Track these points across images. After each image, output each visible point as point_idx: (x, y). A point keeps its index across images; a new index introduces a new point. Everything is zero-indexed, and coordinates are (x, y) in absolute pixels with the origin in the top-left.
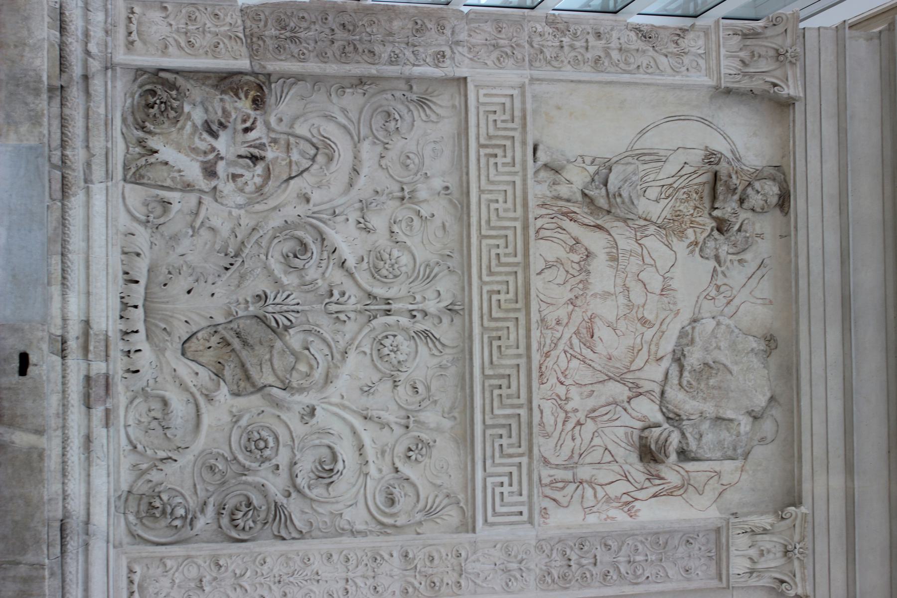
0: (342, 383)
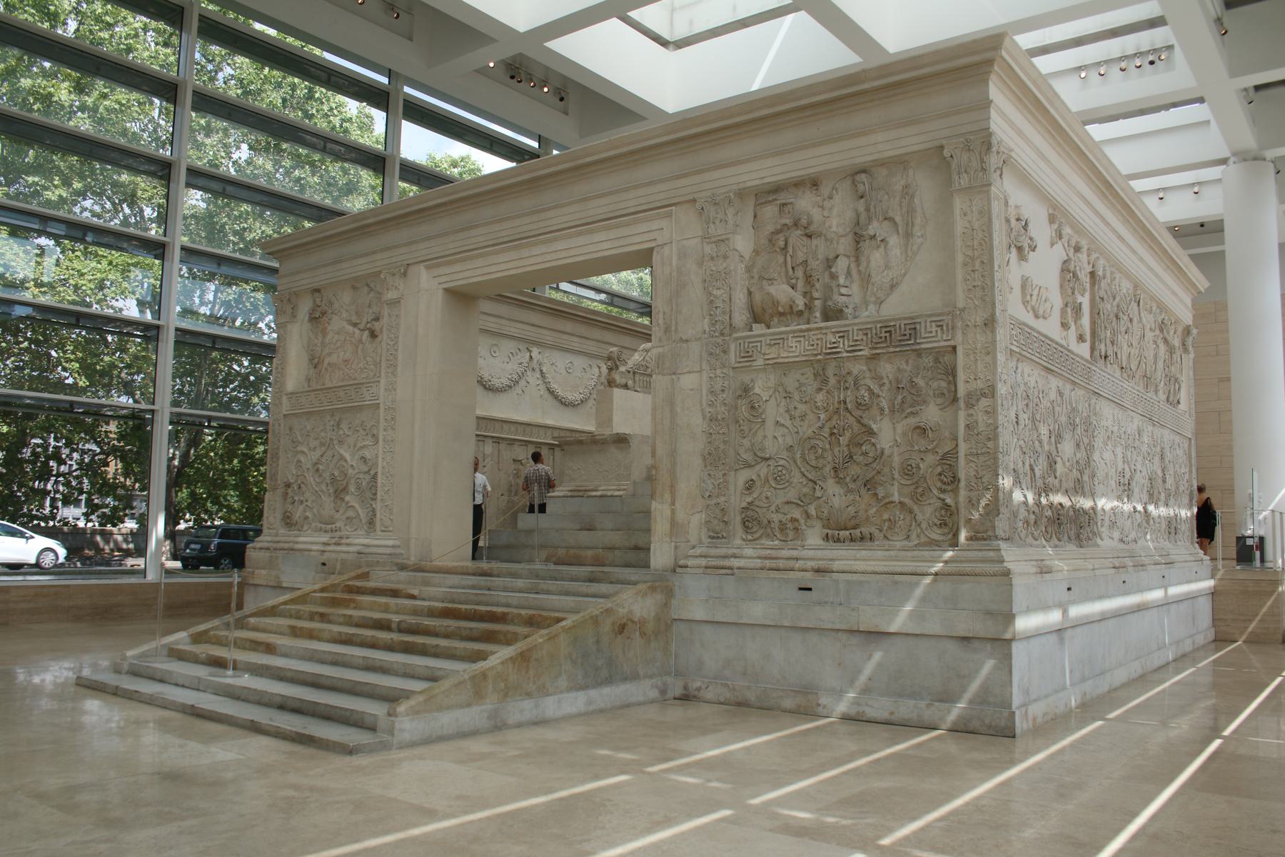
0: (348, 457)
